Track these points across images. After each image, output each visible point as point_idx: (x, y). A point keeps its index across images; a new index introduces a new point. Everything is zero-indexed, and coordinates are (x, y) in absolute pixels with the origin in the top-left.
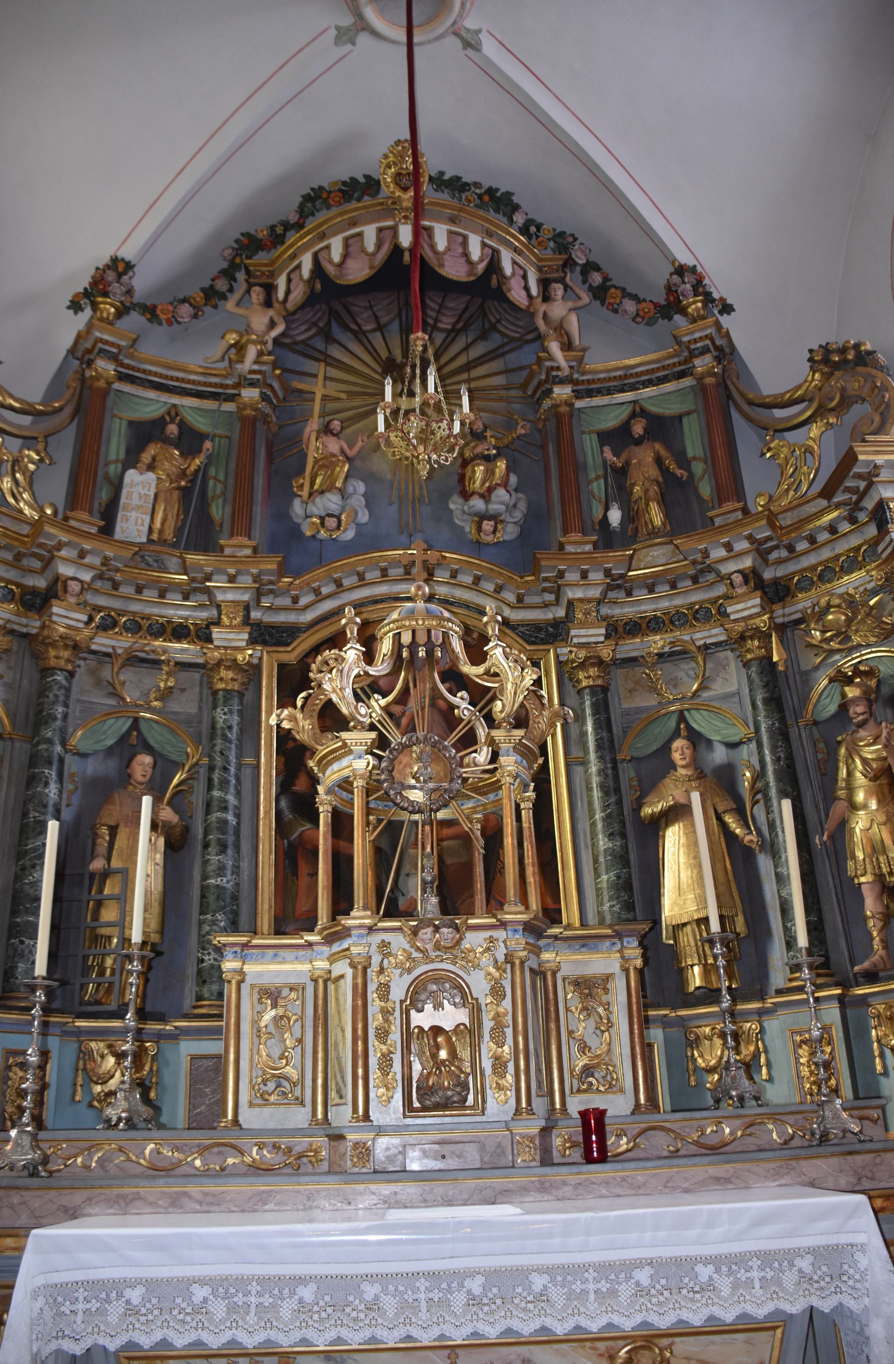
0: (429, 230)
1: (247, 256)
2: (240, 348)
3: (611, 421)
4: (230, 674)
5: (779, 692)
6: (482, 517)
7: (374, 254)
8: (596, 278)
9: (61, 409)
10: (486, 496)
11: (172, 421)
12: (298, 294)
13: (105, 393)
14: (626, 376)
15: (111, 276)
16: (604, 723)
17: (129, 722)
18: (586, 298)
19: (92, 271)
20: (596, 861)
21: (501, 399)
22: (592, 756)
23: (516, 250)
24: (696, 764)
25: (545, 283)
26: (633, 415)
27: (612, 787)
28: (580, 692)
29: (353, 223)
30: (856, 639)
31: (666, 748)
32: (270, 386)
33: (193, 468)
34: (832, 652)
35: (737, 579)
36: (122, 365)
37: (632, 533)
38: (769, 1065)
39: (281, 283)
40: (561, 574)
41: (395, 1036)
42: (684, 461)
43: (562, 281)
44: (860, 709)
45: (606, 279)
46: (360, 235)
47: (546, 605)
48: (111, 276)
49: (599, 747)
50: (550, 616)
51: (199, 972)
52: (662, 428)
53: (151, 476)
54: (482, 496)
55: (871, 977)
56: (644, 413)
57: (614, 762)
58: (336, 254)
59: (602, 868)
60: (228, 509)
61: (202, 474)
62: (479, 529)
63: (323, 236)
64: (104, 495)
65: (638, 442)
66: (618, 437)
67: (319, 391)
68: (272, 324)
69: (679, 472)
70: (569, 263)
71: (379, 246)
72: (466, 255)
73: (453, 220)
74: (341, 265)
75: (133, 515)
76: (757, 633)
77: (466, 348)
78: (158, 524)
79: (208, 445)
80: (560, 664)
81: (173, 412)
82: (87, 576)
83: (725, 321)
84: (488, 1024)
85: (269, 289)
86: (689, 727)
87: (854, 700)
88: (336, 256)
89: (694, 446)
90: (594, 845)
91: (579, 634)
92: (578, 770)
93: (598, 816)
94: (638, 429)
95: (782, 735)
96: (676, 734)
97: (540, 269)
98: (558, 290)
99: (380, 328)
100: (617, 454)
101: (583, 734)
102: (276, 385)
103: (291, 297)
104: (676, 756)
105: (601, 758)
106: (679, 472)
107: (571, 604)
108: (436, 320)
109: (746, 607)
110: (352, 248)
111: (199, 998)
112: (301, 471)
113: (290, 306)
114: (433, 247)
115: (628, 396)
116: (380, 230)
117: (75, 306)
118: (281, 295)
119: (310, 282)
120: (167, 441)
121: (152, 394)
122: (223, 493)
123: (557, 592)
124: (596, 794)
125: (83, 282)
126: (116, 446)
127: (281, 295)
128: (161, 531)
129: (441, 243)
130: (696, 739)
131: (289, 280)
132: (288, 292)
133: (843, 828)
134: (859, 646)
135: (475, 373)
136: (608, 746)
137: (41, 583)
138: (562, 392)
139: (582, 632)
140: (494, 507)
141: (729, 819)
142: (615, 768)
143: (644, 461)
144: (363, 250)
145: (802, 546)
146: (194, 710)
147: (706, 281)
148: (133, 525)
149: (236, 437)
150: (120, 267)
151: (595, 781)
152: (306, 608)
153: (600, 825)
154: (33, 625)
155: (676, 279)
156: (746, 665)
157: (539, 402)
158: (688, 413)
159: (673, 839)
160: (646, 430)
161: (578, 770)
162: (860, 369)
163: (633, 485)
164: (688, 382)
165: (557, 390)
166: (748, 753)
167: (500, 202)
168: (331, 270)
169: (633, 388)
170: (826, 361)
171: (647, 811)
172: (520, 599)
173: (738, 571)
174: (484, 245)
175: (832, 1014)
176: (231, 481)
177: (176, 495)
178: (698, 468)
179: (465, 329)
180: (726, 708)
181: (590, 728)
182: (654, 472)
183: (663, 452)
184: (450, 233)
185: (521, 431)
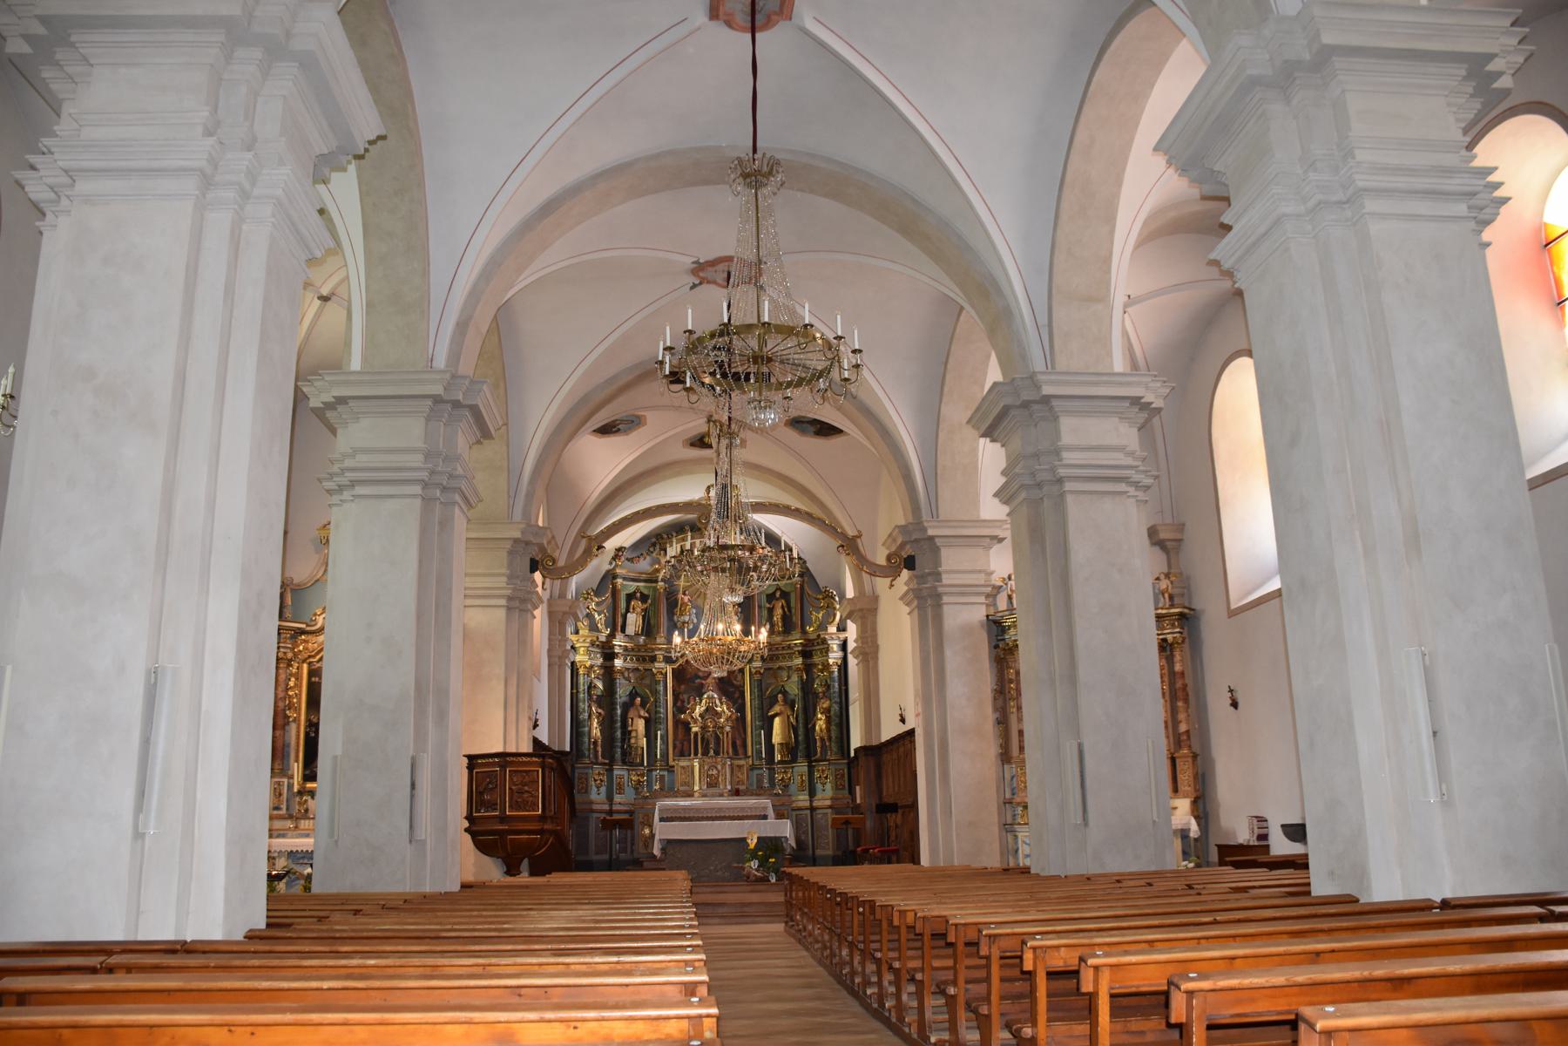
24: (785, 701)
27: (761, 708)
81: (638, 589)
109: (799, 661)
126: (623, 604)
130: (785, 693)
136: (761, 696)
148: (630, 630)
159: (777, 720)
180: (793, 688)
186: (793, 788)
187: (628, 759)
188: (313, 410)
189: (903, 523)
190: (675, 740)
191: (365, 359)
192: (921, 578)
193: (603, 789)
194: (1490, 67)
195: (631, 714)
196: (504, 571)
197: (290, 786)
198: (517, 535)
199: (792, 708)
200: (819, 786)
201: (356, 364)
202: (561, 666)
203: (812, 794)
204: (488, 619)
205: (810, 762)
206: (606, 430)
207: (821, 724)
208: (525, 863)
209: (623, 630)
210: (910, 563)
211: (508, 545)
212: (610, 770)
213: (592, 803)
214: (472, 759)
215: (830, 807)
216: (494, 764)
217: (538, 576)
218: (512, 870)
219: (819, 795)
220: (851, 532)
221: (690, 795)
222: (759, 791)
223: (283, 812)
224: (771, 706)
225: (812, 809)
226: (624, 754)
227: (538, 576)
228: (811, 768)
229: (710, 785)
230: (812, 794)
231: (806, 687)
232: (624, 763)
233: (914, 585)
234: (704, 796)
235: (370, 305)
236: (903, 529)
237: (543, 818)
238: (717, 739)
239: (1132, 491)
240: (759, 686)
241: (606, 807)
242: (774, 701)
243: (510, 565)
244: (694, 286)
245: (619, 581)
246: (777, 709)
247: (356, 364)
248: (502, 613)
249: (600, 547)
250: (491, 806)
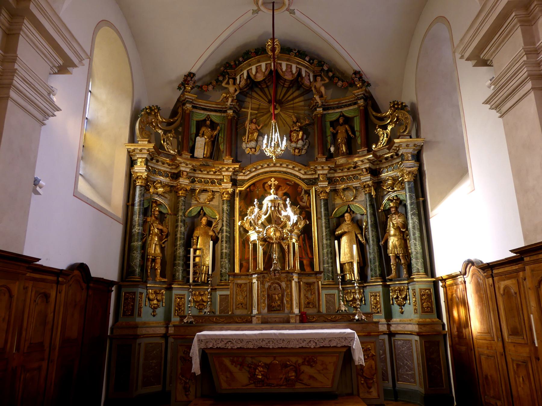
0: (281, 64)
1: (226, 69)
2: (227, 98)
3: (334, 118)
4: (227, 196)
5: (375, 203)
6: (296, 148)
7: (264, 73)
8: (331, 74)
9: (177, 119)
10: (297, 142)
11: (208, 120)
12: (243, 83)
13: (189, 114)
14: (339, 104)
15: (189, 79)
16: (326, 209)
17: (200, 208)
18: (327, 81)
19: (183, 77)
20: (323, 245)
21: (302, 110)
22: (323, 218)
23: (307, 67)
25: (315, 77)
26: (340, 116)
28: (320, 200)
29: (259, 62)
30: (396, 189)
31: (343, 216)
32: (235, 108)
33: (215, 134)
34: (389, 192)
35: (364, 170)
36: (193, 103)
37: (338, 152)
38: (365, 301)
39: (238, 77)
40: (316, 167)
41: (266, 296)
42: (354, 132)
43: (320, 76)
44: (393, 209)
45: (334, 74)
46: (260, 66)
47: (312, 174)
48: (189, 79)
49: (325, 215)
50: (314, 177)
51: (221, 274)
52: (348, 121)
53: (203, 138)
54: (295, 142)
55: (391, 280)
56: (343, 116)
57: (329, 219)
58: (254, 71)
59: (325, 248)
60: (225, 146)
61: (217, 136)
62: (295, 151)
63: (250, 65)
64: (191, 144)
65: (341, 125)
66: (334, 124)
67: (249, 111)
68: (236, 90)
69: (352, 135)
70: (323, 70)
71: (266, 70)
72: (291, 71)
73: (288, 60)
74: (255, 75)
75: (199, 150)
76: (369, 186)
77: (292, 93)
78: (205, 152)
79: (218, 128)
80: (316, 191)
82: (188, 170)
83: (369, 89)
84: (285, 293)
85: (235, 80)
86: (351, 210)
87: (392, 207)
88: (254, 73)
89: (357, 127)
90: (323, 242)
91: (321, 184)
92: (319, 220)
93: (324, 234)
94: (341, 121)
95: (374, 214)
96: (347, 212)
97: (314, 72)
98: (319, 79)
99: (267, 87)
100: (334, 129)
101: (321, 212)
102: (237, 107)
103: (241, 83)
104: (346, 218)
105: (325, 219)
106: (352, 135)
107: (319, 175)
108: (284, 84)
109: (367, 178)
110: (258, 69)
111: (221, 280)
112: (245, 134)
113: (241, 86)
114: (281, 70)
115: (339, 110)
116: (266, 64)
117: (179, 88)
118: (238, 82)
119: (246, 80)
120: (206, 126)
121: (202, 112)
122: (223, 142)
123: (315, 171)
124: (324, 228)
125: (182, 80)
126: (193, 130)
127: (238, 82)
128: (207, 154)
129: (284, 68)
131: (240, 78)
132: (240, 82)
133: (387, 242)
134: (396, 191)
135: (295, 101)
136: (328, 215)
137: (176, 171)
138: (320, 110)
139: (322, 183)
140: (299, 146)
141: (359, 236)
142: (329, 221)
143: (341, 130)
144: (261, 70)
145: (384, 161)
146: (217, 204)
147: (363, 76)
149: (226, 124)
150: (191, 75)
151: (324, 225)
152: (246, 175)
153: (324, 237)
154: (175, 183)
155: (354, 76)
156: (366, 194)
157: (313, 112)
158: (356, 116)
160: (344, 121)
161: (319, 220)
162: (403, 111)
163: (339, 139)
164: (356, 106)
165: (318, 109)
166: (365, 217)
167: (302, 54)
168: (252, 76)
169: (341, 107)
170: (393, 106)
171: (337, 233)
172: (305, 173)
173: (365, 168)
174: (297, 67)
175: (380, 289)
176: (225, 138)
177: (210, 143)
178: (357, 134)
179: (292, 87)
181: (323, 210)
182: (345, 135)
183: (348, 128)
184: (287, 65)
185: (307, 122)
190: (241, 261)
193: (160, 311)
195: (197, 233)
200: (396, 308)
203: (389, 316)
205: (384, 280)
207: (393, 241)
209: (192, 150)
212: (169, 289)
213: (136, 327)
215: (418, 334)
219: (396, 319)
222: (346, 319)
225: (391, 335)
228: (386, 287)
229: (270, 309)
241: (162, 331)
242: (340, 219)
245: (189, 106)
246: (344, 228)
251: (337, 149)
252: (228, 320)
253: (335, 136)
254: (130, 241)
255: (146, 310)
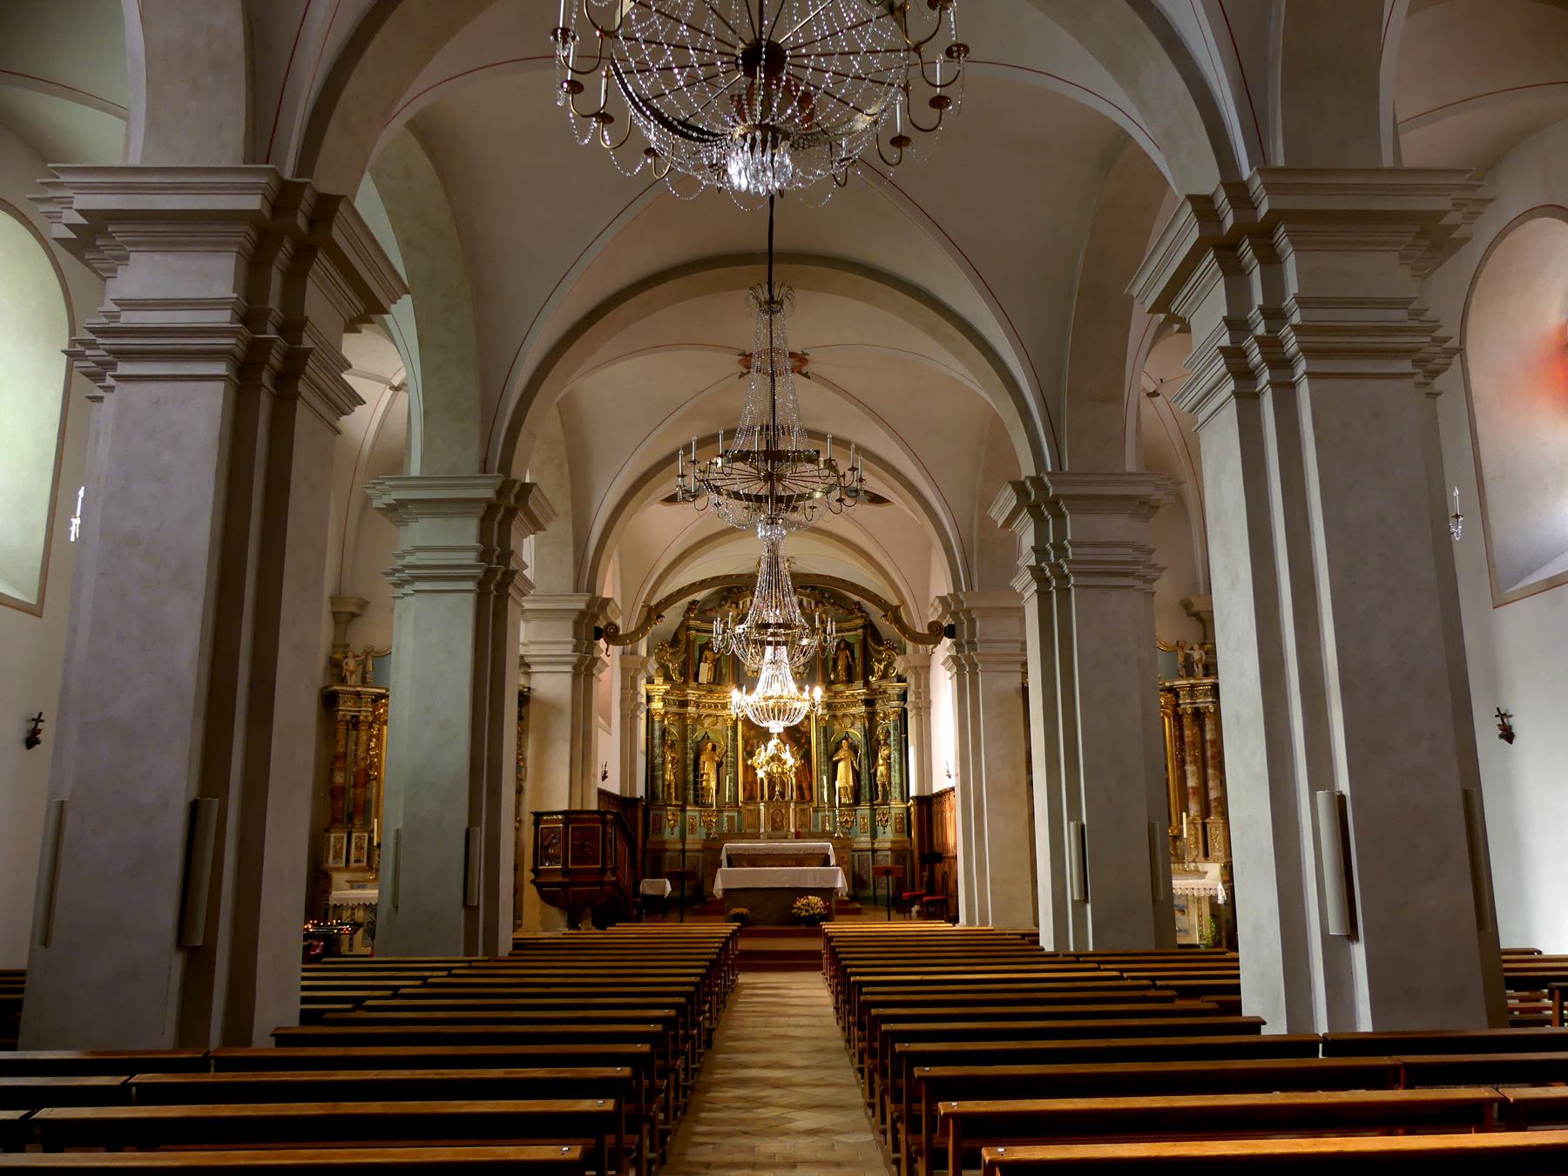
89: (857, 655)
109: (861, 709)
136: (826, 742)
159: (841, 766)
180: (857, 733)
186: (857, 829)
187: (699, 798)
188: (378, 509)
189: (945, 594)
191: (423, 463)
192: (958, 646)
193: (677, 830)
194: (1444, 221)
195: (703, 758)
196: (570, 639)
197: (371, 840)
198: (582, 606)
199: (856, 753)
200: (880, 829)
201: (415, 469)
202: (634, 717)
203: (874, 836)
204: (552, 684)
206: (672, 499)
207: (881, 769)
208: (589, 911)
209: (696, 679)
210: (950, 632)
211: (574, 616)
212: (683, 810)
213: (664, 842)
214: (538, 816)
216: (557, 821)
217: (602, 643)
218: (573, 924)
219: (880, 836)
220: (895, 602)
221: (756, 837)
223: (364, 864)
224: (837, 750)
225: (874, 851)
226: (696, 796)
227: (602, 643)
228: (873, 810)
230: (874, 836)
231: (870, 734)
232: (696, 803)
233: (953, 652)
234: (770, 837)
235: (426, 413)
236: (942, 600)
237: (603, 871)
238: (783, 784)
239: (1139, 584)
240: (826, 732)
241: (680, 846)
242: (838, 747)
243: (576, 635)
244: (742, 375)
246: (841, 754)
247: (415, 469)
248: (568, 679)
249: (659, 616)
250: (553, 859)
251: (837, 675)
252: (743, 836)
253: (835, 661)
254: (653, 770)
255: (668, 829)
